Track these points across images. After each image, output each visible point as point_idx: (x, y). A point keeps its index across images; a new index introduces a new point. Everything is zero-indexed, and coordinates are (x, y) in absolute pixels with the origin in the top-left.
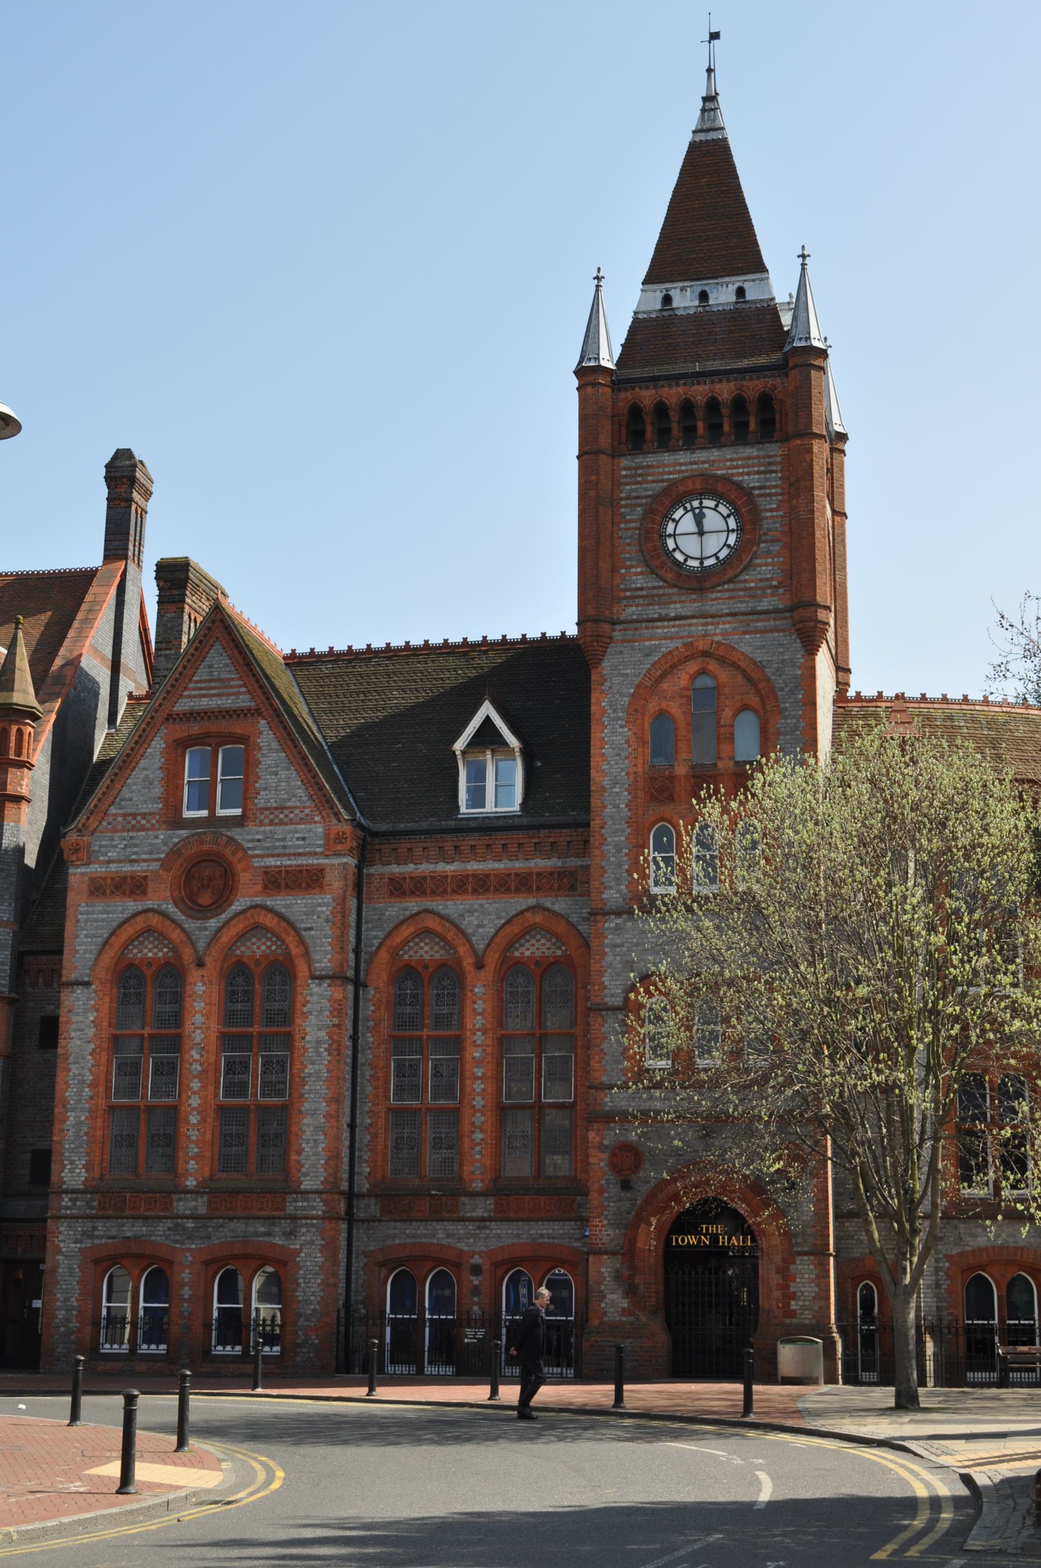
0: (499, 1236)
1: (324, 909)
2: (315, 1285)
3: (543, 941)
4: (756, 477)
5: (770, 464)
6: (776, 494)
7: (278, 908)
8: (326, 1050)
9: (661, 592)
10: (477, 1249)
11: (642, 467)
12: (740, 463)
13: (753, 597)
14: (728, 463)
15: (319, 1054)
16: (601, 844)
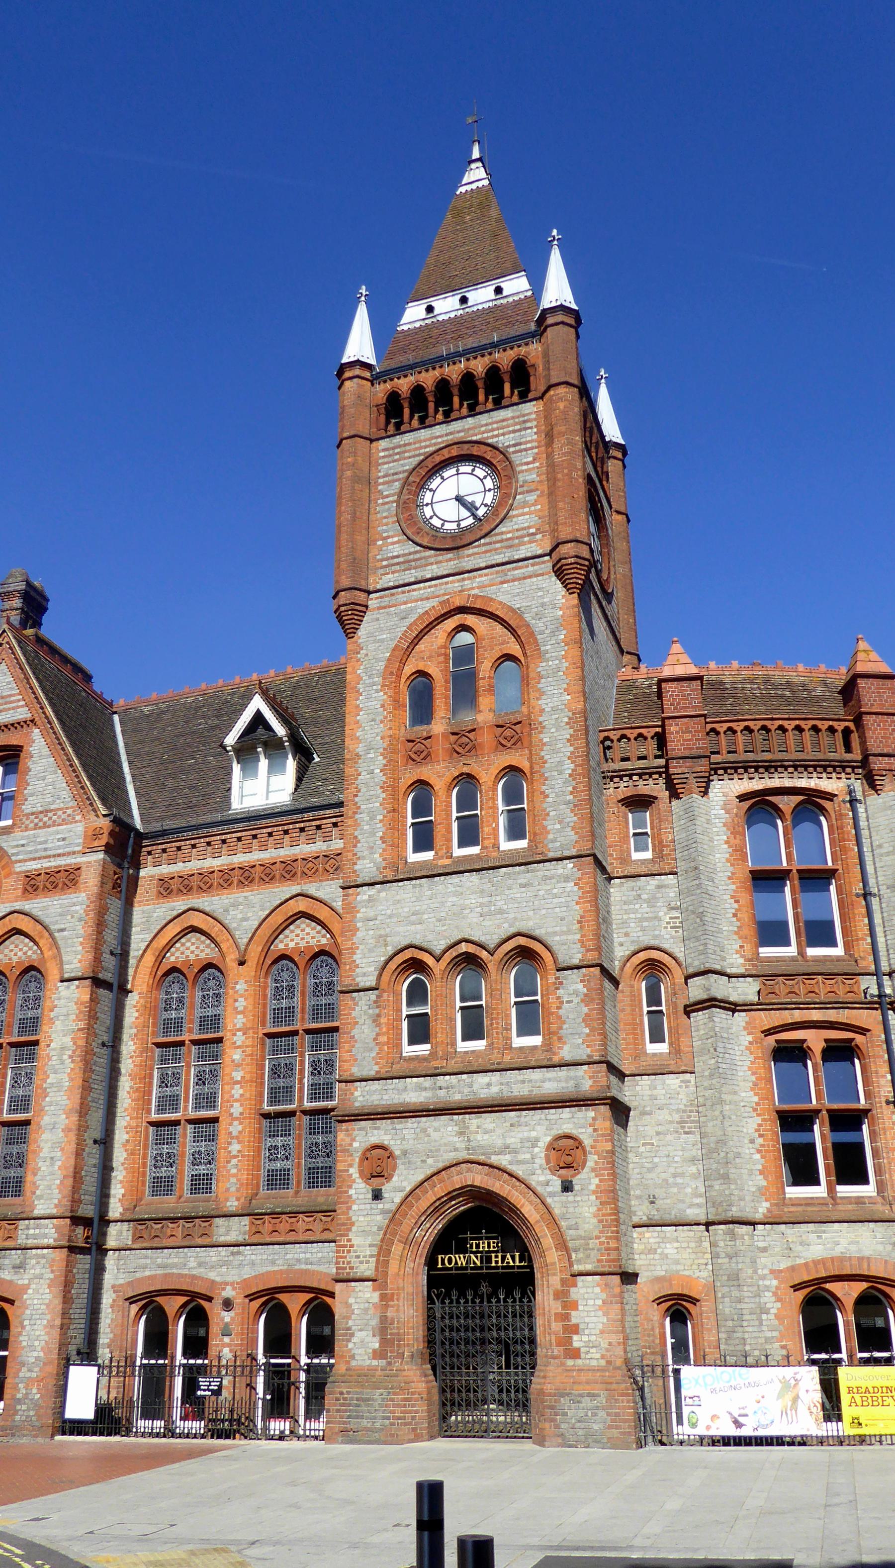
0: (253, 1264)
1: (78, 908)
2: (41, 1327)
3: (308, 930)
4: (512, 435)
5: (524, 422)
6: (532, 448)
7: (36, 912)
8: (70, 1057)
9: (418, 556)
10: (229, 1279)
11: (400, 446)
12: (495, 426)
13: (510, 547)
14: (483, 429)
15: (62, 1062)
16: (355, 813)
